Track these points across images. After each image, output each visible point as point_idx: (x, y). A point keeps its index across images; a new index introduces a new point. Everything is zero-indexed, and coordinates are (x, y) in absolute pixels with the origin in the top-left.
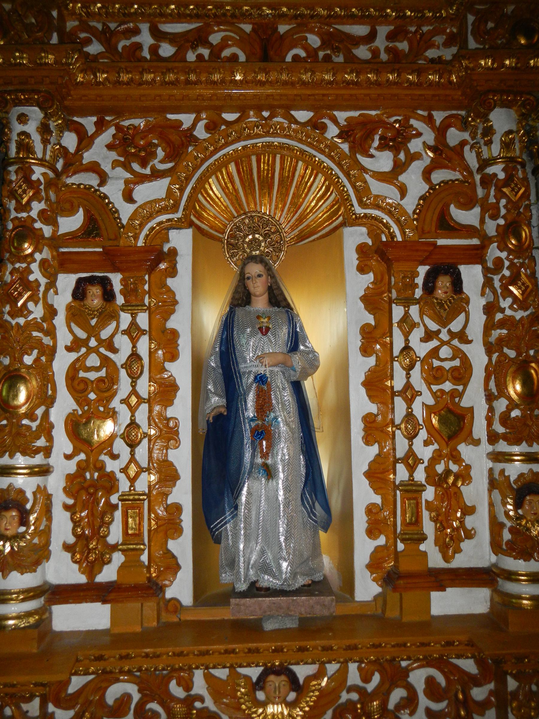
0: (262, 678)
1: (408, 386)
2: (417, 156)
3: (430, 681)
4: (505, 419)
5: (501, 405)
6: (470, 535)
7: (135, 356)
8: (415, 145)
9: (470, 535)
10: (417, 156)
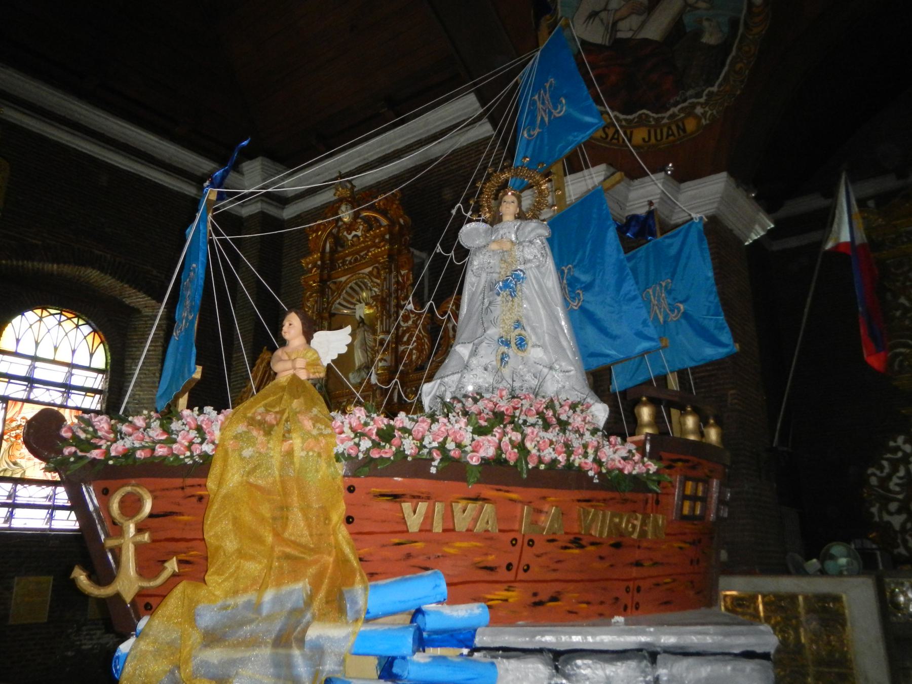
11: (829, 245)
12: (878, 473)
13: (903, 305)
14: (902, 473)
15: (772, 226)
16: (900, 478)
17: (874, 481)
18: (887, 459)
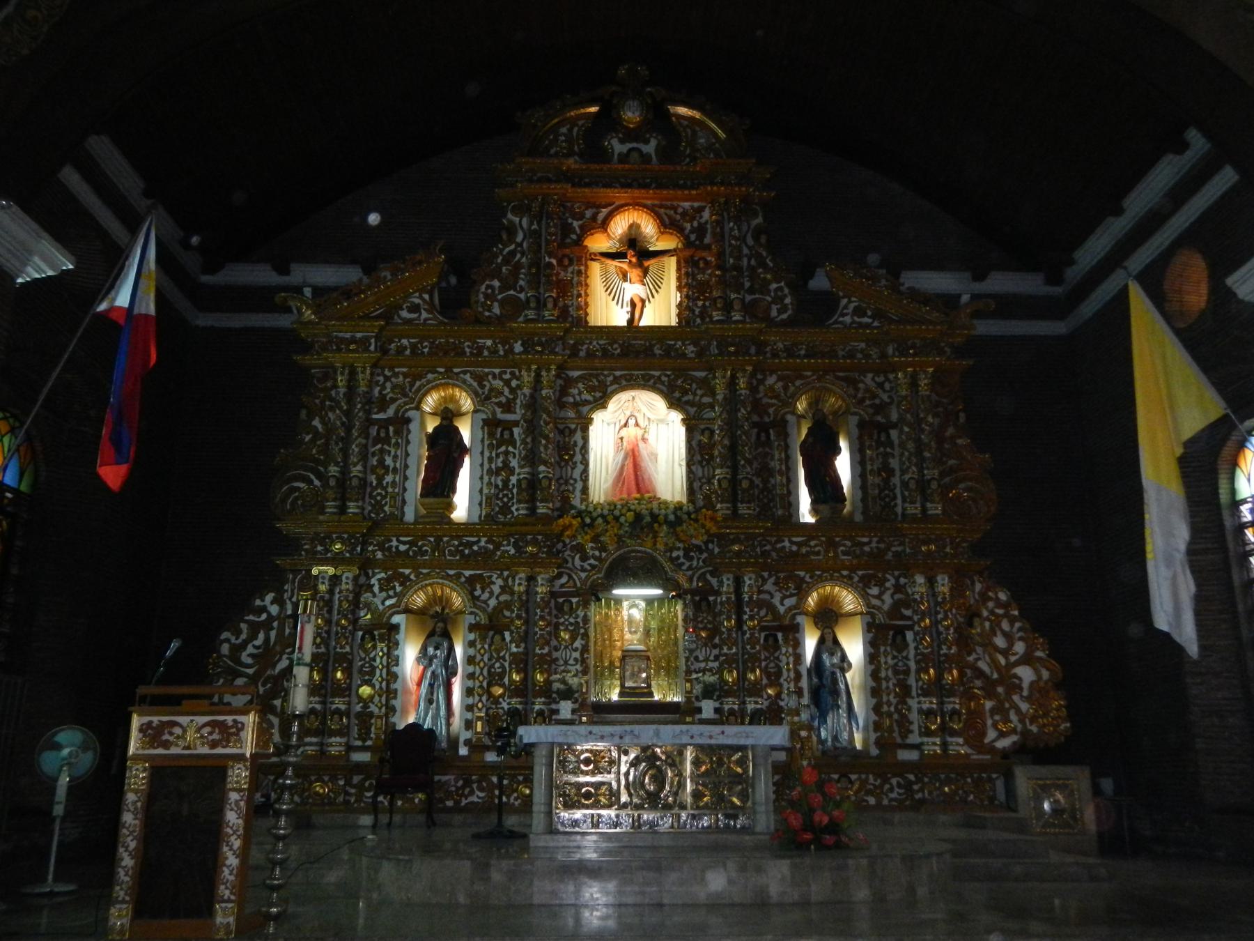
0: (839, 778)
1: (887, 676)
2: (889, 589)
3: (898, 783)
4: (922, 688)
5: (920, 683)
6: (912, 732)
7: (788, 664)
8: (888, 585)
9: (912, 732)
10: (889, 589)
11: (103, 307)
12: (233, 640)
13: (316, 427)
14: (258, 642)
15: (71, 267)
16: (255, 647)
17: (225, 649)
18: (246, 622)
